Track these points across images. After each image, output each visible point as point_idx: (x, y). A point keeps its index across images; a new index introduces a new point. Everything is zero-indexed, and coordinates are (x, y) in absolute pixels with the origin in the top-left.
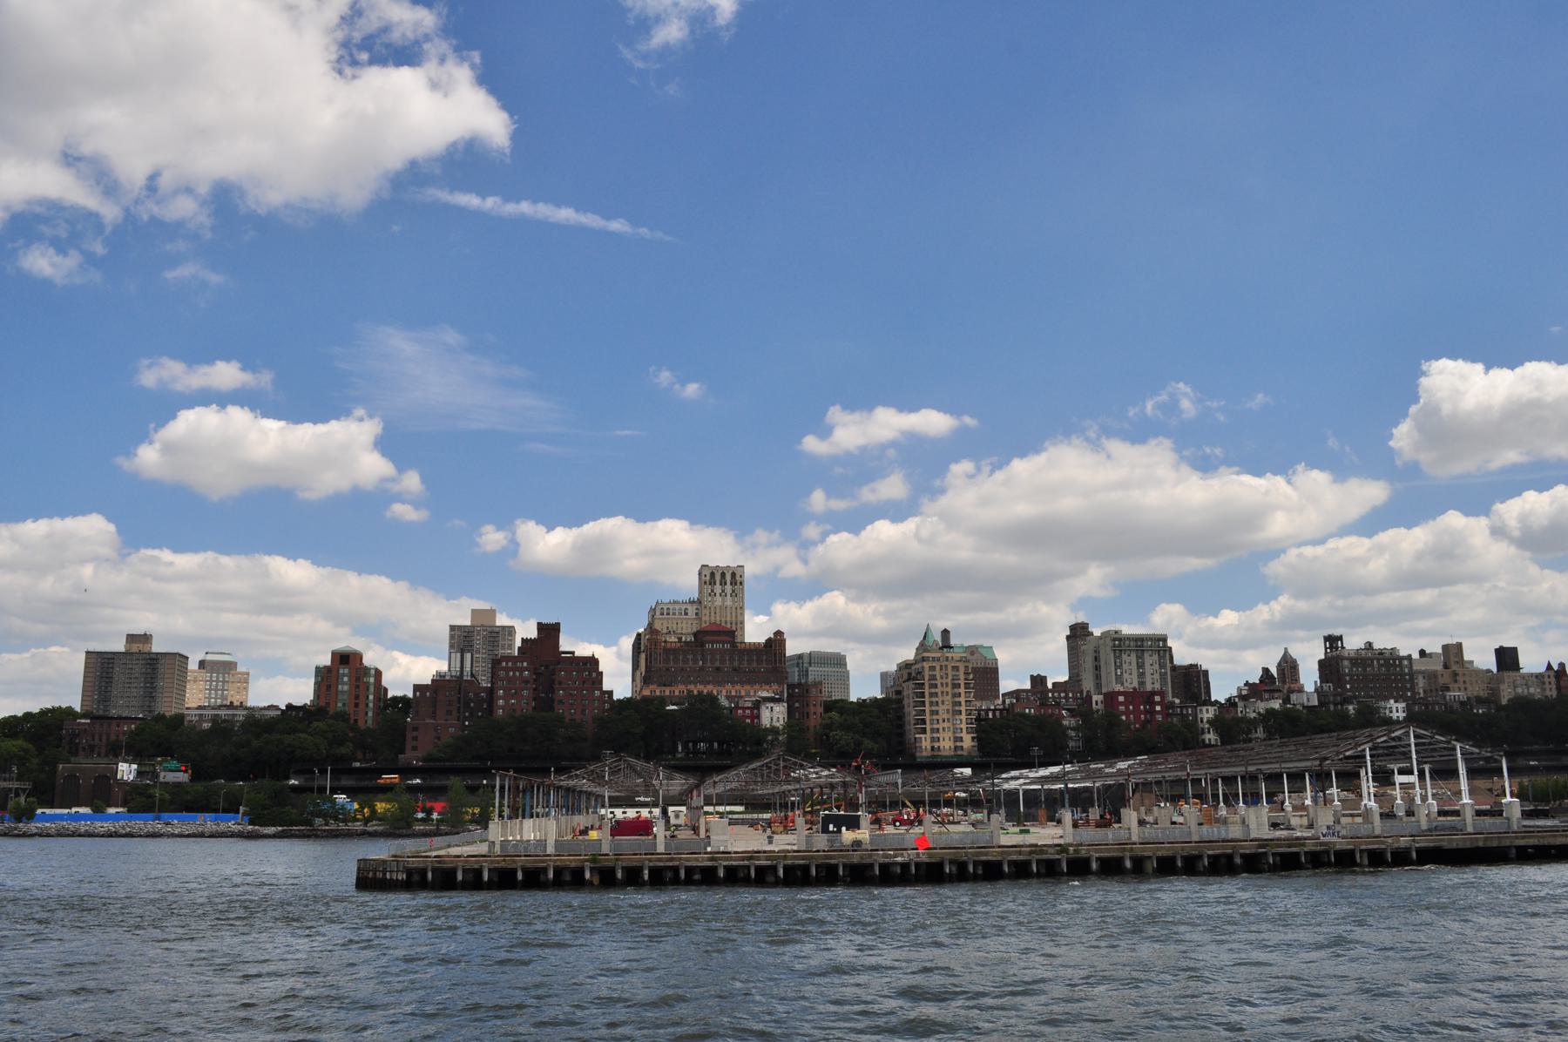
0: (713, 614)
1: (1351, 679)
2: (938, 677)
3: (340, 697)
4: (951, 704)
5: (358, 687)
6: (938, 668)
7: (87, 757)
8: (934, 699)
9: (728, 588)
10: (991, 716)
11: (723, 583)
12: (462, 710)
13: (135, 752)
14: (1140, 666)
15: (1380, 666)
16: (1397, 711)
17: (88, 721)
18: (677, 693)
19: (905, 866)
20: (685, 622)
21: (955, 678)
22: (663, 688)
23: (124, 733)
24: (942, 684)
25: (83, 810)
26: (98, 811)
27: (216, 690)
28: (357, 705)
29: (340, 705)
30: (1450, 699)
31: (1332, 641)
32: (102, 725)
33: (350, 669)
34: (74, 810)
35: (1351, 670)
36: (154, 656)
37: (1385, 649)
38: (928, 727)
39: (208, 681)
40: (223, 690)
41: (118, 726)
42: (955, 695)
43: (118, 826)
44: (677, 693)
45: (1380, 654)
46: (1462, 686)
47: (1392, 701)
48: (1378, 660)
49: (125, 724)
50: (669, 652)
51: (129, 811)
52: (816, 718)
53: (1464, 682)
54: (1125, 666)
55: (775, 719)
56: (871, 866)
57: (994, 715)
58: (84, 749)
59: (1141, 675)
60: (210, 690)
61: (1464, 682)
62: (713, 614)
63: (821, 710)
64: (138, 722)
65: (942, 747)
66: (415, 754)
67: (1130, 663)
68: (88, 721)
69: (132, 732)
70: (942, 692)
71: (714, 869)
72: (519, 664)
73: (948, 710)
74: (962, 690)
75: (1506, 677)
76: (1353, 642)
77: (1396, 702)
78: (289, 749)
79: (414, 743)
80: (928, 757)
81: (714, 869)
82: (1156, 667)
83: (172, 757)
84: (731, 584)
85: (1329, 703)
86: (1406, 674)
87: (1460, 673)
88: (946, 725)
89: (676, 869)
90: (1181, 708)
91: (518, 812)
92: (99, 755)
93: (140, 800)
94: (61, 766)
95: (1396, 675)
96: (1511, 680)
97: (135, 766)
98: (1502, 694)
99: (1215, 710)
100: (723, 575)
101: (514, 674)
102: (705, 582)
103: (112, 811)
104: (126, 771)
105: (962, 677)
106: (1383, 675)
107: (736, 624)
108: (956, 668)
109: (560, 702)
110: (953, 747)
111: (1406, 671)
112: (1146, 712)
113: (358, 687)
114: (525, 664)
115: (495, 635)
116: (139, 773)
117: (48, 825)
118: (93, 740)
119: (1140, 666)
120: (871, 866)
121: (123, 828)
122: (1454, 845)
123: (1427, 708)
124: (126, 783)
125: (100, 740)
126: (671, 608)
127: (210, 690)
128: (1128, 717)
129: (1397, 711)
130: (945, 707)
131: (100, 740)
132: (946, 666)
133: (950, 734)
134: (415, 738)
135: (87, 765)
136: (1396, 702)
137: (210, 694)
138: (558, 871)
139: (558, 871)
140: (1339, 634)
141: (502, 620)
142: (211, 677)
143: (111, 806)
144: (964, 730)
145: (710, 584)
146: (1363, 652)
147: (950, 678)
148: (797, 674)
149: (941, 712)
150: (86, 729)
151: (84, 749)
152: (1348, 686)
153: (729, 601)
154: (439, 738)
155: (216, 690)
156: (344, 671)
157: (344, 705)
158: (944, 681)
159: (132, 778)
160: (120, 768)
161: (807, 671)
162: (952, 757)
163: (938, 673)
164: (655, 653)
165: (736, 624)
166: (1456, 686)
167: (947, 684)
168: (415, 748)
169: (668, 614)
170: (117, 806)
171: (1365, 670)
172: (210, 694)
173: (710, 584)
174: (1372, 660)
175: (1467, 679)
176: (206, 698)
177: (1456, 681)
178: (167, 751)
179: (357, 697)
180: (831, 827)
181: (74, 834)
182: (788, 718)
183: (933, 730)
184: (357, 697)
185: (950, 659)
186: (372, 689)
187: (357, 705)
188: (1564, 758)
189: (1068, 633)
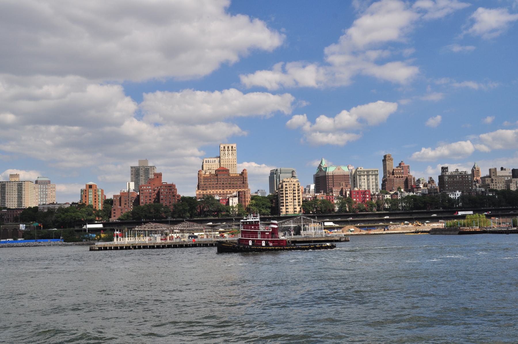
0: (225, 162)
1: (448, 183)
2: (288, 188)
3: (89, 199)
4: (292, 196)
5: (95, 196)
6: (288, 185)
7: (7, 222)
8: (286, 195)
9: (230, 152)
10: (309, 200)
11: (228, 150)
12: (130, 203)
13: (23, 221)
14: (368, 180)
15: (459, 178)
16: (458, 195)
17: (6, 210)
18: (208, 193)
19: (190, 245)
20: (214, 165)
21: (294, 188)
22: (203, 191)
23: (19, 214)
24: (289, 190)
25: (10, 240)
26: (15, 239)
27: (43, 192)
28: (95, 202)
29: (90, 202)
30: (478, 191)
31: (444, 169)
32: (11, 212)
33: (93, 190)
34: (8, 240)
35: (448, 179)
36: (21, 183)
37: (462, 172)
38: (285, 204)
39: (39, 188)
40: (46, 192)
41: (16, 212)
42: (294, 194)
43: (22, 244)
44: (208, 193)
45: (460, 173)
46: (495, 184)
47: (458, 191)
48: (459, 176)
49: (19, 211)
50: (205, 178)
51: (25, 239)
52: (248, 202)
53: (496, 183)
54: (363, 181)
55: (234, 203)
56: (183, 245)
57: (311, 199)
58: (6, 220)
59: (368, 184)
60: (41, 192)
61: (496, 183)
62: (225, 162)
63: (250, 199)
64: (23, 210)
65: (289, 211)
66: (114, 218)
67: (364, 179)
68: (6, 210)
69: (21, 214)
70: (290, 193)
71: (154, 246)
72: (148, 187)
73: (291, 199)
74: (296, 192)
75: (513, 181)
76: (452, 169)
77: (459, 192)
78: (73, 218)
79: (114, 215)
80: (285, 215)
81: (154, 246)
82: (374, 180)
83: (36, 221)
84: (231, 150)
85: (432, 193)
86: (470, 181)
87: (494, 179)
88: (291, 204)
89: (147, 246)
90: (377, 195)
91: (123, 236)
92: (11, 221)
93: (28, 236)
94: (1, 226)
95: (465, 181)
96: (515, 182)
97: (25, 225)
98: (511, 187)
99: (390, 196)
100: (228, 147)
101: (146, 191)
102: (222, 150)
103: (19, 239)
104: (22, 227)
105: (296, 187)
106: (461, 181)
107: (234, 165)
108: (294, 184)
109: (162, 199)
110: (293, 211)
111: (470, 179)
112: (363, 197)
113: (95, 196)
114: (150, 187)
115: (148, 170)
116: (26, 227)
117: (4, 244)
118: (8, 216)
119: (368, 180)
120: (183, 245)
121: (27, 244)
122: (299, 240)
123: (469, 194)
124: (23, 231)
125: (11, 217)
126: (209, 160)
127: (41, 192)
128: (356, 200)
129: (458, 195)
130: (291, 198)
131: (11, 217)
132: (291, 184)
133: (292, 207)
134: (114, 213)
135: (9, 225)
136: (459, 192)
137: (41, 193)
138: (126, 247)
139: (126, 247)
140: (446, 166)
141: (150, 164)
142: (41, 187)
143: (19, 238)
144: (297, 205)
145: (223, 151)
146: (454, 173)
147: (292, 188)
148: (275, 177)
149: (289, 199)
150: (6, 213)
151: (6, 220)
152: (447, 186)
153: (231, 157)
154: (122, 213)
155: (43, 192)
156: (91, 190)
157: (91, 202)
158: (290, 189)
159: (24, 229)
160: (20, 226)
161: (279, 176)
162: (293, 214)
163: (288, 186)
164: (201, 179)
165: (234, 165)
166: (492, 184)
167: (291, 190)
168: (114, 216)
169: (208, 162)
170: (21, 238)
171: (454, 180)
172: (41, 193)
173: (223, 151)
174: (456, 176)
175: (497, 182)
176: (39, 195)
177: (492, 182)
178: (34, 220)
179: (95, 199)
180: (190, 238)
181: (13, 246)
182: (238, 202)
183: (286, 206)
184: (95, 199)
185: (293, 181)
186: (100, 196)
187: (95, 202)
188: (517, 211)
189: (383, 159)
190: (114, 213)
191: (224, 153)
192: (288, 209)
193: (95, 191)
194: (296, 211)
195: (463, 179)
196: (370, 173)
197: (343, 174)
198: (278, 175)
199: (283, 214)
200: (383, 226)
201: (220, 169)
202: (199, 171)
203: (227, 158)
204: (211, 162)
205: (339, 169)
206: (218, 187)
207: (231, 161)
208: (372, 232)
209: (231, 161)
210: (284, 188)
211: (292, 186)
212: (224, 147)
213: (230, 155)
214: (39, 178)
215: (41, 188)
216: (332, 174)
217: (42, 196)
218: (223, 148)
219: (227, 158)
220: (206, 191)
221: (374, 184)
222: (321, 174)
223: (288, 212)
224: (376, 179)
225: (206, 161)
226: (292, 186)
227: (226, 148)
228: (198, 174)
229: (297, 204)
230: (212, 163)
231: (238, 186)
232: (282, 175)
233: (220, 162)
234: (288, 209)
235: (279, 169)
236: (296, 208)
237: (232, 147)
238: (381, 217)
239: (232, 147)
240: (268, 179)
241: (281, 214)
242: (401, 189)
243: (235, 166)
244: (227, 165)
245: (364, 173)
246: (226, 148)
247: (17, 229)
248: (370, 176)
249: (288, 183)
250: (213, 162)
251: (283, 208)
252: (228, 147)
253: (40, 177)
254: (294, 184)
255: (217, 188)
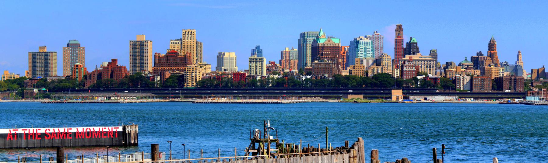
2: (189, 70)
5: (80, 72)
9: (190, 36)
22: (157, 68)
36: (47, 53)
39: (71, 51)
66: (87, 87)
104: (36, 91)
108: (193, 69)
128: (236, 79)
134: (87, 84)
147: (192, 71)
158: (190, 71)
163: (189, 70)
166: (354, 70)
168: (87, 86)
177: (355, 68)
178: (44, 87)
190: (87, 84)
191: (185, 37)
192: (188, 84)
193: (80, 69)
194: (193, 86)
195: (326, 66)
196: (258, 60)
197: (333, 45)
198: (305, 39)
199: (185, 87)
200: (242, 97)
201: (170, 52)
202: (155, 54)
203: (187, 40)
204: (175, 43)
205: (329, 41)
206: (168, 65)
207: (190, 43)
208: (175, 100)
209: (190, 43)
210: (186, 71)
211: (192, 70)
212: (185, 32)
213: (190, 38)
214: (70, 42)
215: (72, 51)
216: (322, 46)
217: (73, 58)
218: (184, 33)
219: (187, 40)
220: (159, 68)
221: (260, 67)
222: (315, 45)
223: (188, 86)
224: (262, 64)
225: (172, 42)
226: (192, 70)
227: (187, 33)
228: (155, 55)
229: (194, 81)
230: (176, 44)
231: (179, 64)
232: (309, 39)
233: (181, 43)
234: (188, 84)
235: (306, 33)
236: (193, 84)
237: (191, 32)
238: (232, 91)
239: (191, 32)
240: (298, 41)
241: (184, 87)
242: (106, 88)
243: (193, 47)
244: (187, 46)
245: (253, 60)
246: (187, 33)
247: (32, 92)
248: (258, 62)
249: (189, 68)
250: (177, 43)
251: (185, 83)
252: (188, 32)
253: (71, 41)
254: (193, 69)
255: (167, 66)
